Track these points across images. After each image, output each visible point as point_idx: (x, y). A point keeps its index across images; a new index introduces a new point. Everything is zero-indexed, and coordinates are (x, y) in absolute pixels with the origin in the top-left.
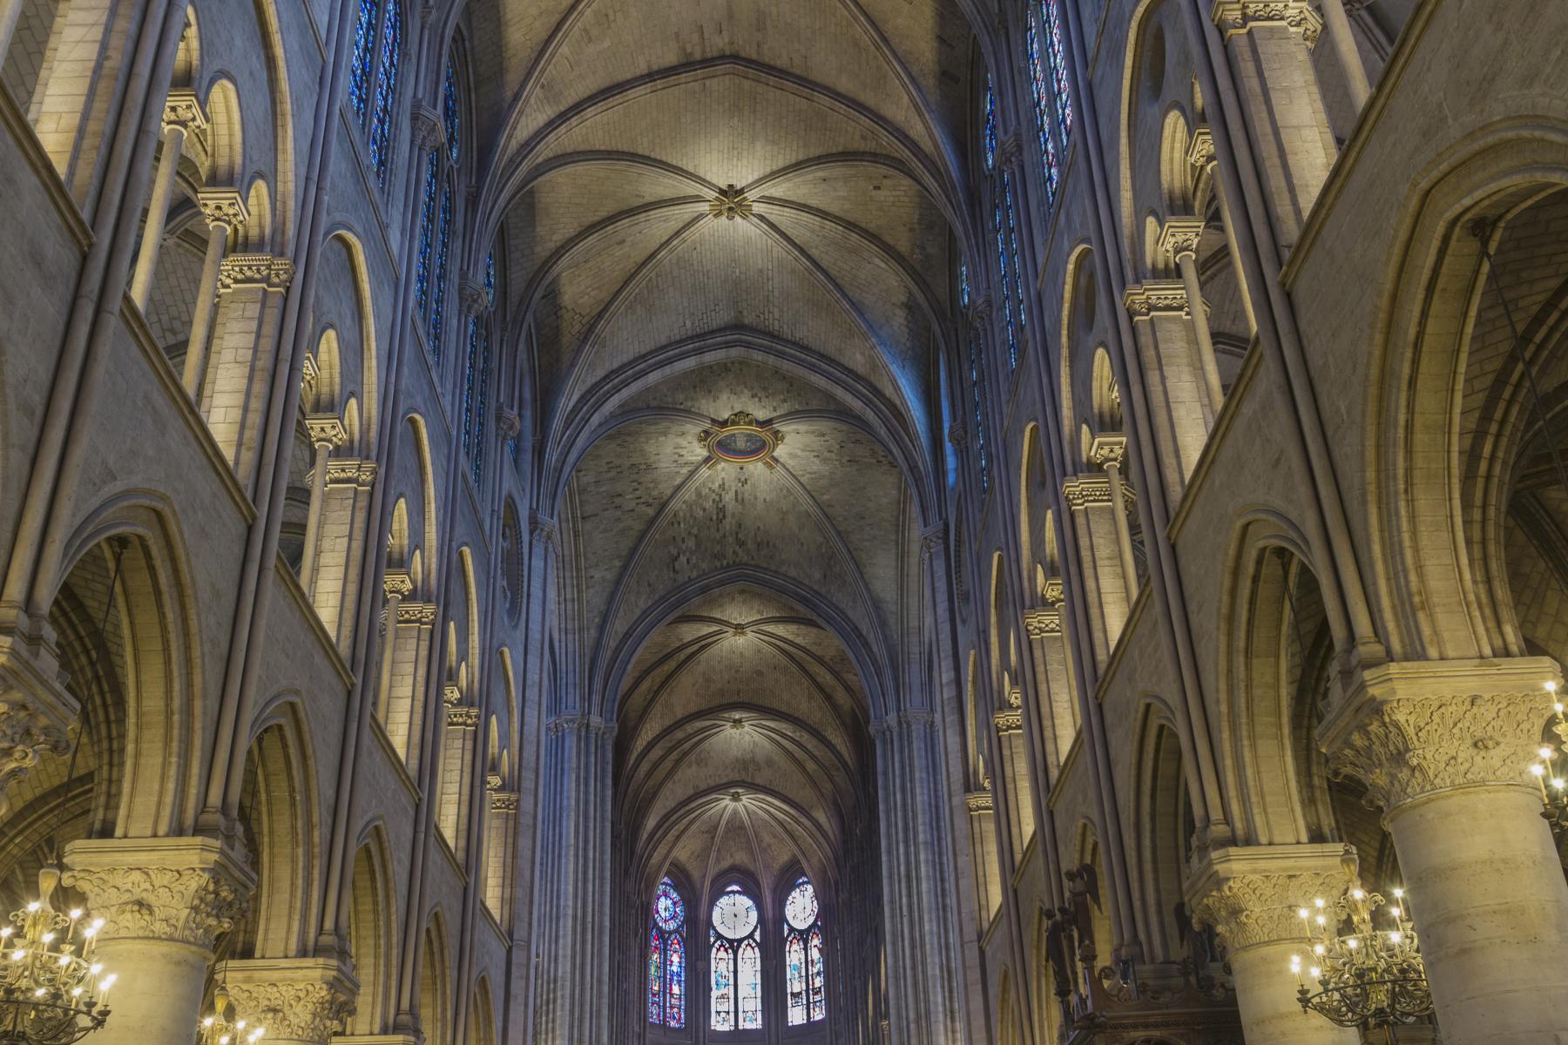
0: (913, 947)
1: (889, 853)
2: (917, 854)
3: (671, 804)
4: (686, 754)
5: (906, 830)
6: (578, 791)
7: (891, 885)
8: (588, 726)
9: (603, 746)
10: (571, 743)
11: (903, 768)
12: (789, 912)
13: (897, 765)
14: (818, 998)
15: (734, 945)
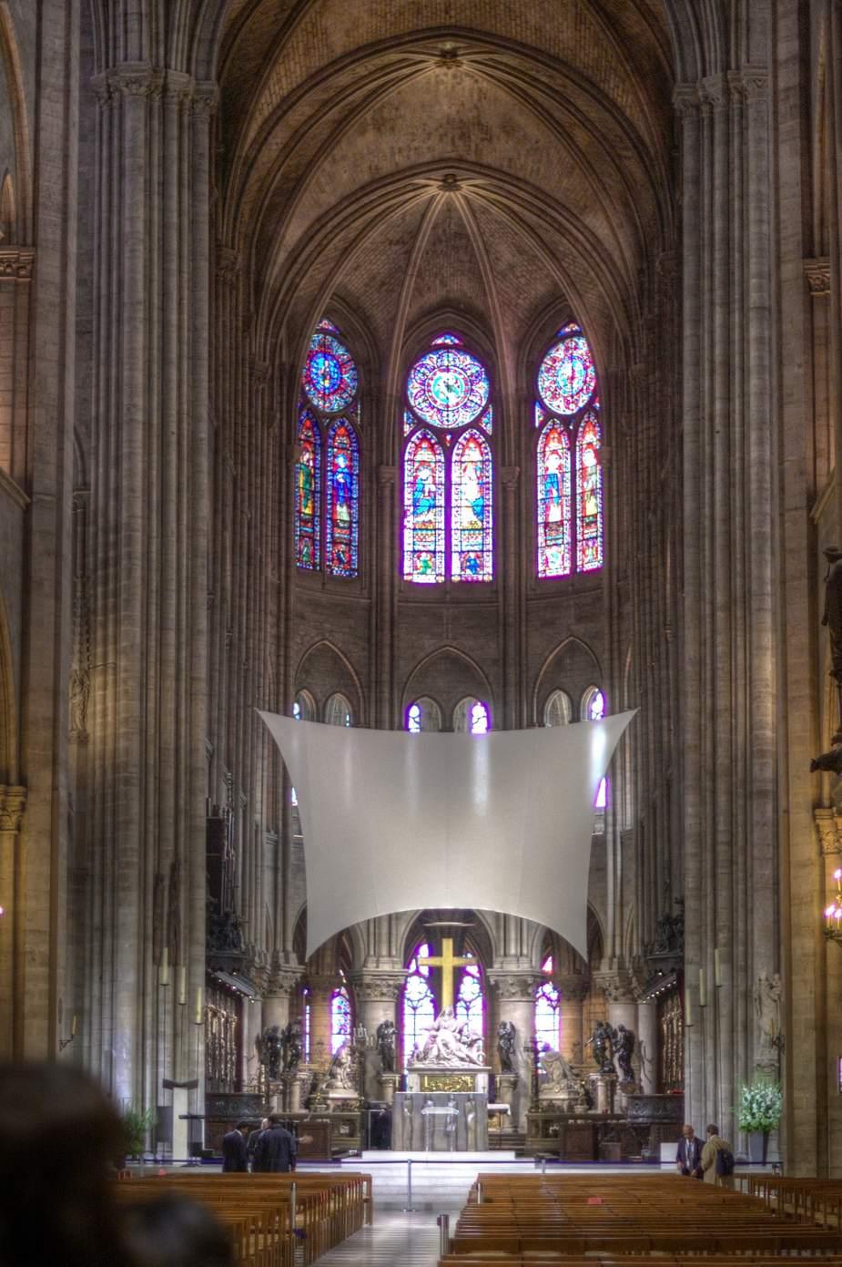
0: (729, 485)
1: (697, 322)
2: (744, 328)
3: (329, 199)
4: (353, 111)
5: (728, 284)
6: (149, 208)
7: (697, 378)
8: (165, 89)
9: (193, 125)
10: (134, 119)
11: (728, 172)
12: (544, 382)
13: (718, 168)
14: (590, 532)
15: (445, 440)
